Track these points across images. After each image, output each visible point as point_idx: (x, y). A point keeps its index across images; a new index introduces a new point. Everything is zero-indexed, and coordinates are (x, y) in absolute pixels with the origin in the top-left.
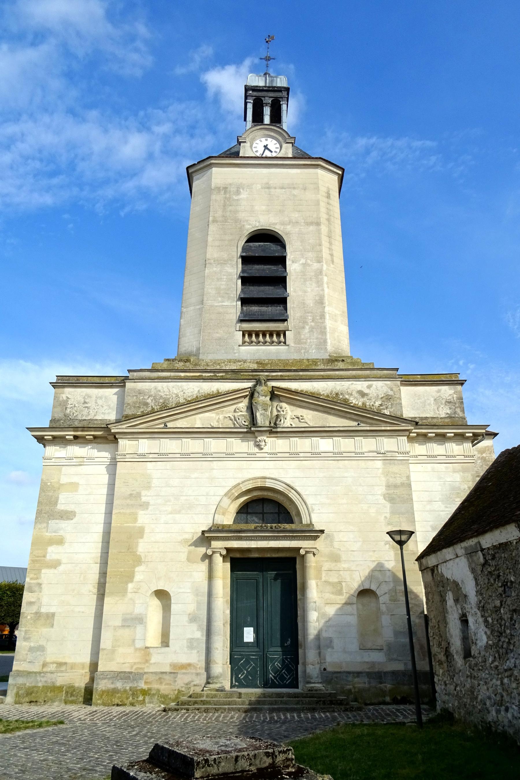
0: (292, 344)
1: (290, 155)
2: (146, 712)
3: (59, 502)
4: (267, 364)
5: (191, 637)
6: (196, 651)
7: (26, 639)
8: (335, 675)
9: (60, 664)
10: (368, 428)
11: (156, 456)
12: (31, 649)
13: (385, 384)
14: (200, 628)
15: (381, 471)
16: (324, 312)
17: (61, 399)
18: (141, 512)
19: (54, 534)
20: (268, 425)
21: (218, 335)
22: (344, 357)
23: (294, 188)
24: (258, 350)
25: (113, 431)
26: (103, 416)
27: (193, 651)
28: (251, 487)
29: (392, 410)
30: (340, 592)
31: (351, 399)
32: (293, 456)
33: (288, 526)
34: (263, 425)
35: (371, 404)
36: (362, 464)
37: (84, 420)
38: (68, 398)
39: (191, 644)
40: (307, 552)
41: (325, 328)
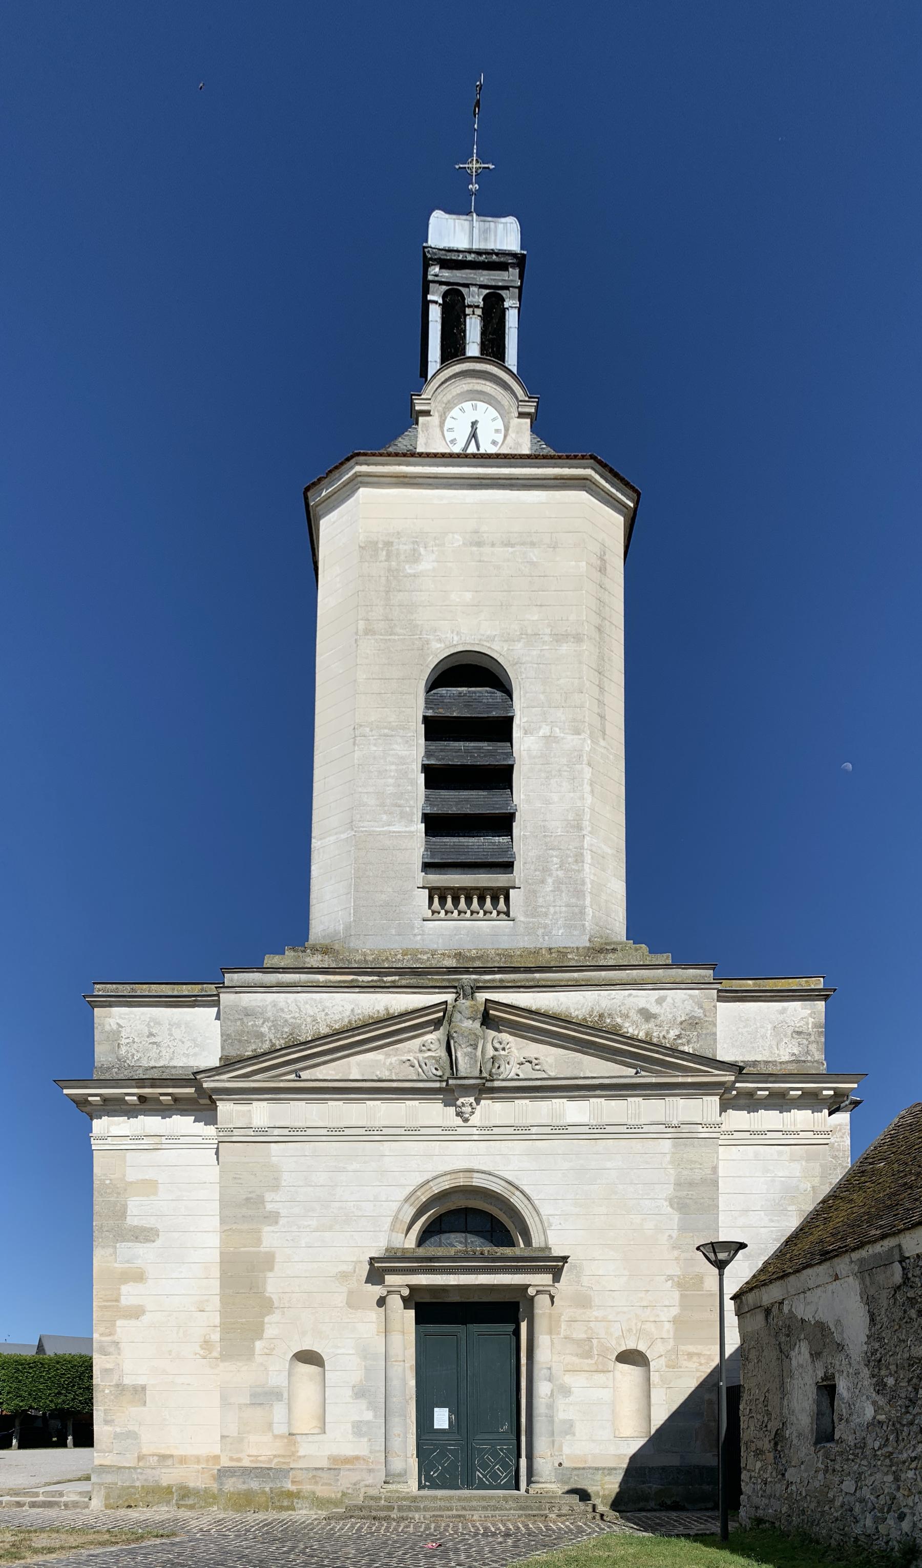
0: (521, 918)
1: (526, 451)
2: (296, 1522)
3: (129, 1213)
4: (473, 959)
5: (358, 1419)
6: (366, 1439)
7: (107, 1422)
8: (575, 1472)
9: (163, 1457)
10: (654, 1080)
11: (286, 1132)
12: (117, 1436)
13: (690, 996)
14: (372, 1406)
15: (668, 1157)
16: (582, 848)
17: (107, 1028)
18: (267, 1229)
19: (127, 1265)
20: (478, 1075)
21: (383, 896)
22: (614, 943)
23: (533, 544)
24: (457, 929)
25: (205, 1085)
26: (184, 1059)
27: (362, 1439)
28: (448, 1187)
29: (697, 1046)
30: (588, 1355)
31: (627, 1025)
32: (520, 1132)
33: (508, 1251)
34: (469, 1075)
35: (661, 1035)
36: (637, 1145)
37: (152, 1068)
38: (120, 1026)
39: (359, 1428)
40: (538, 1292)
41: (583, 883)
